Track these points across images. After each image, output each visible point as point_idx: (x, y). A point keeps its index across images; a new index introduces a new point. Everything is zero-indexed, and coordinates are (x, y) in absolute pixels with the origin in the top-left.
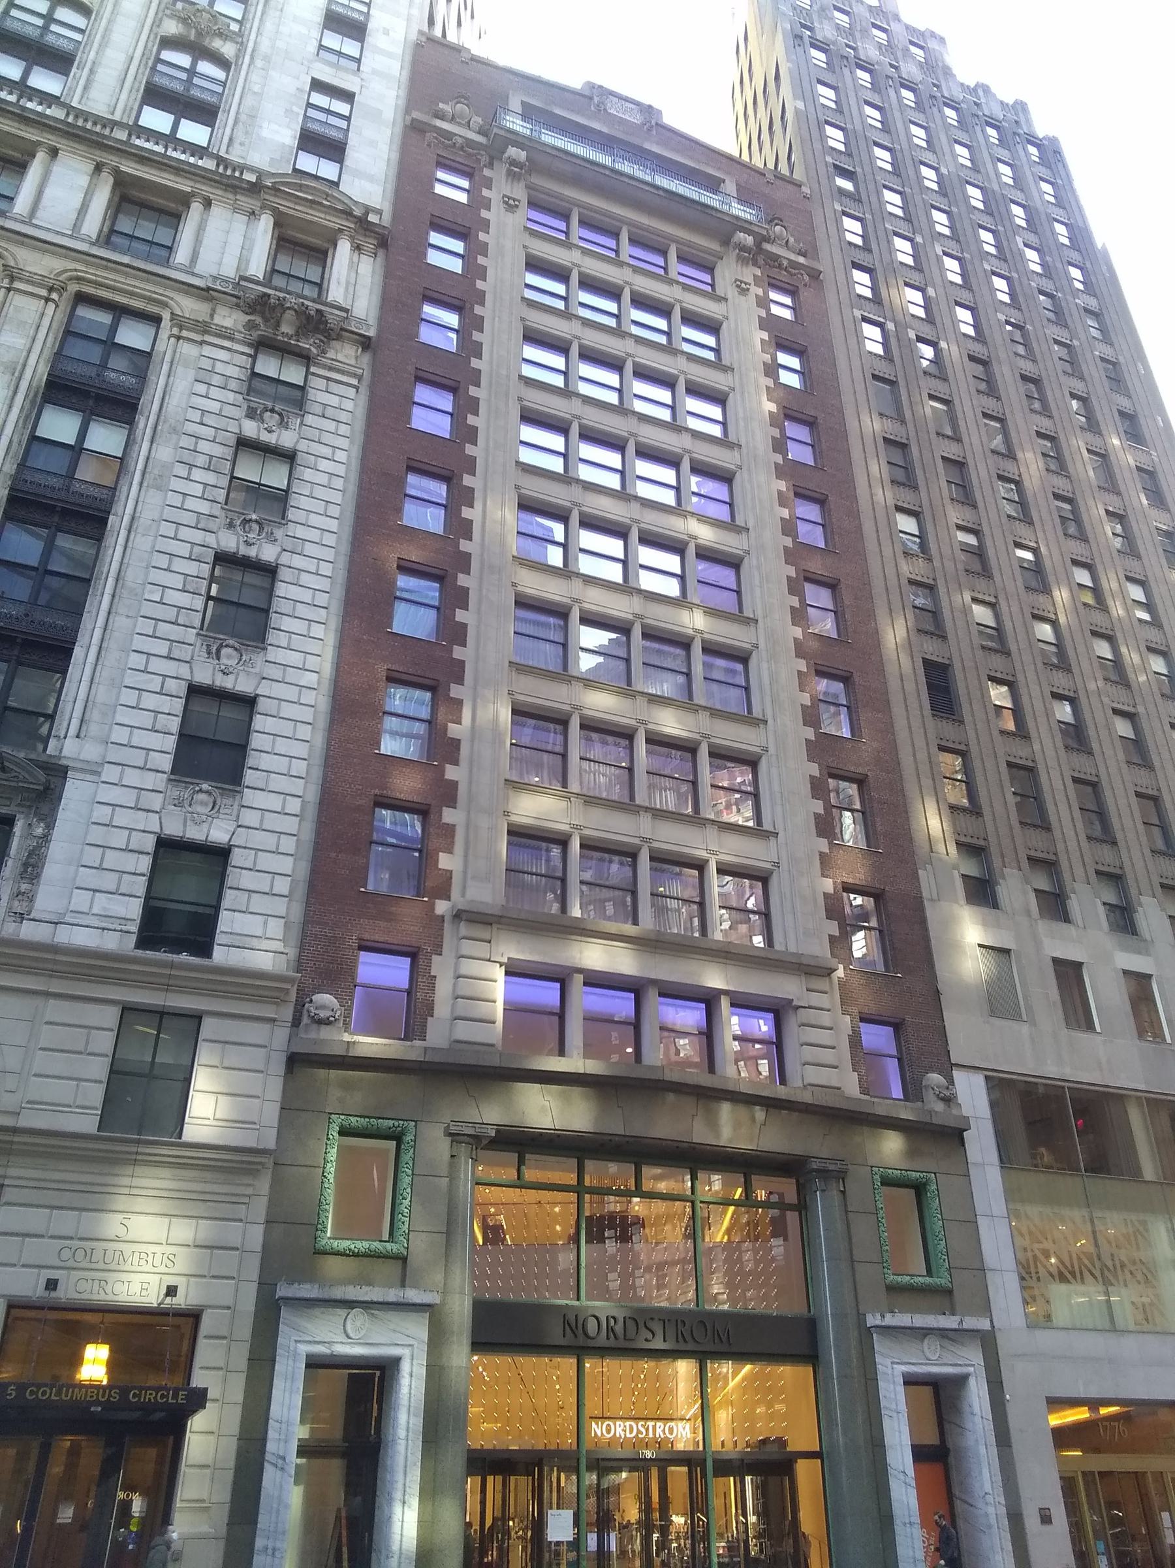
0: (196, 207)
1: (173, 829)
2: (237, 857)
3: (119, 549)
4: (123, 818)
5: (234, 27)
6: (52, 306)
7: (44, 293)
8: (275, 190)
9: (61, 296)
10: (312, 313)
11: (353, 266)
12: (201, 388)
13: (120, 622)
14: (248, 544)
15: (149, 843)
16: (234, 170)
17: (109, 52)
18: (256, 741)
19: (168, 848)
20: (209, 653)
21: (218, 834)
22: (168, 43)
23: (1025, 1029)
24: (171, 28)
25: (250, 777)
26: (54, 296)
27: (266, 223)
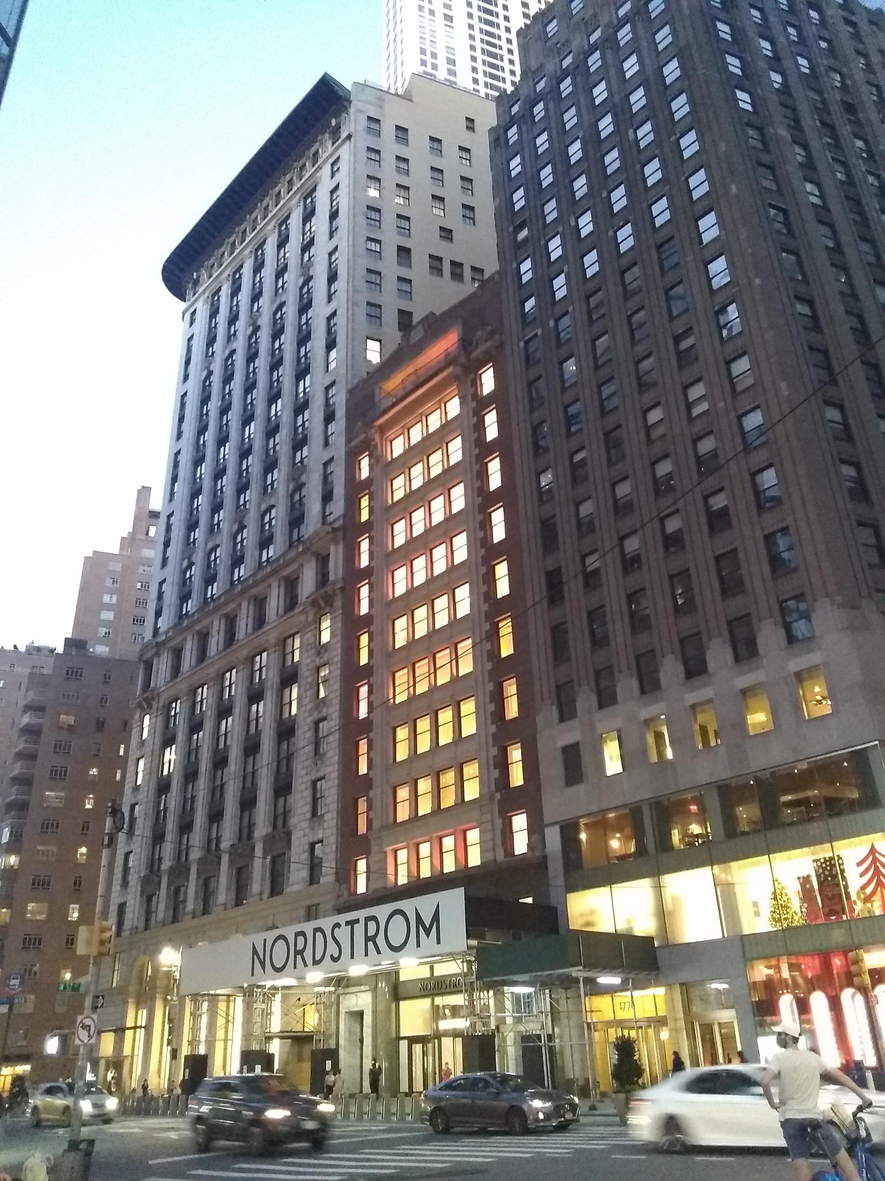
7: (274, 649)
24: (291, 487)
27: (314, 560)
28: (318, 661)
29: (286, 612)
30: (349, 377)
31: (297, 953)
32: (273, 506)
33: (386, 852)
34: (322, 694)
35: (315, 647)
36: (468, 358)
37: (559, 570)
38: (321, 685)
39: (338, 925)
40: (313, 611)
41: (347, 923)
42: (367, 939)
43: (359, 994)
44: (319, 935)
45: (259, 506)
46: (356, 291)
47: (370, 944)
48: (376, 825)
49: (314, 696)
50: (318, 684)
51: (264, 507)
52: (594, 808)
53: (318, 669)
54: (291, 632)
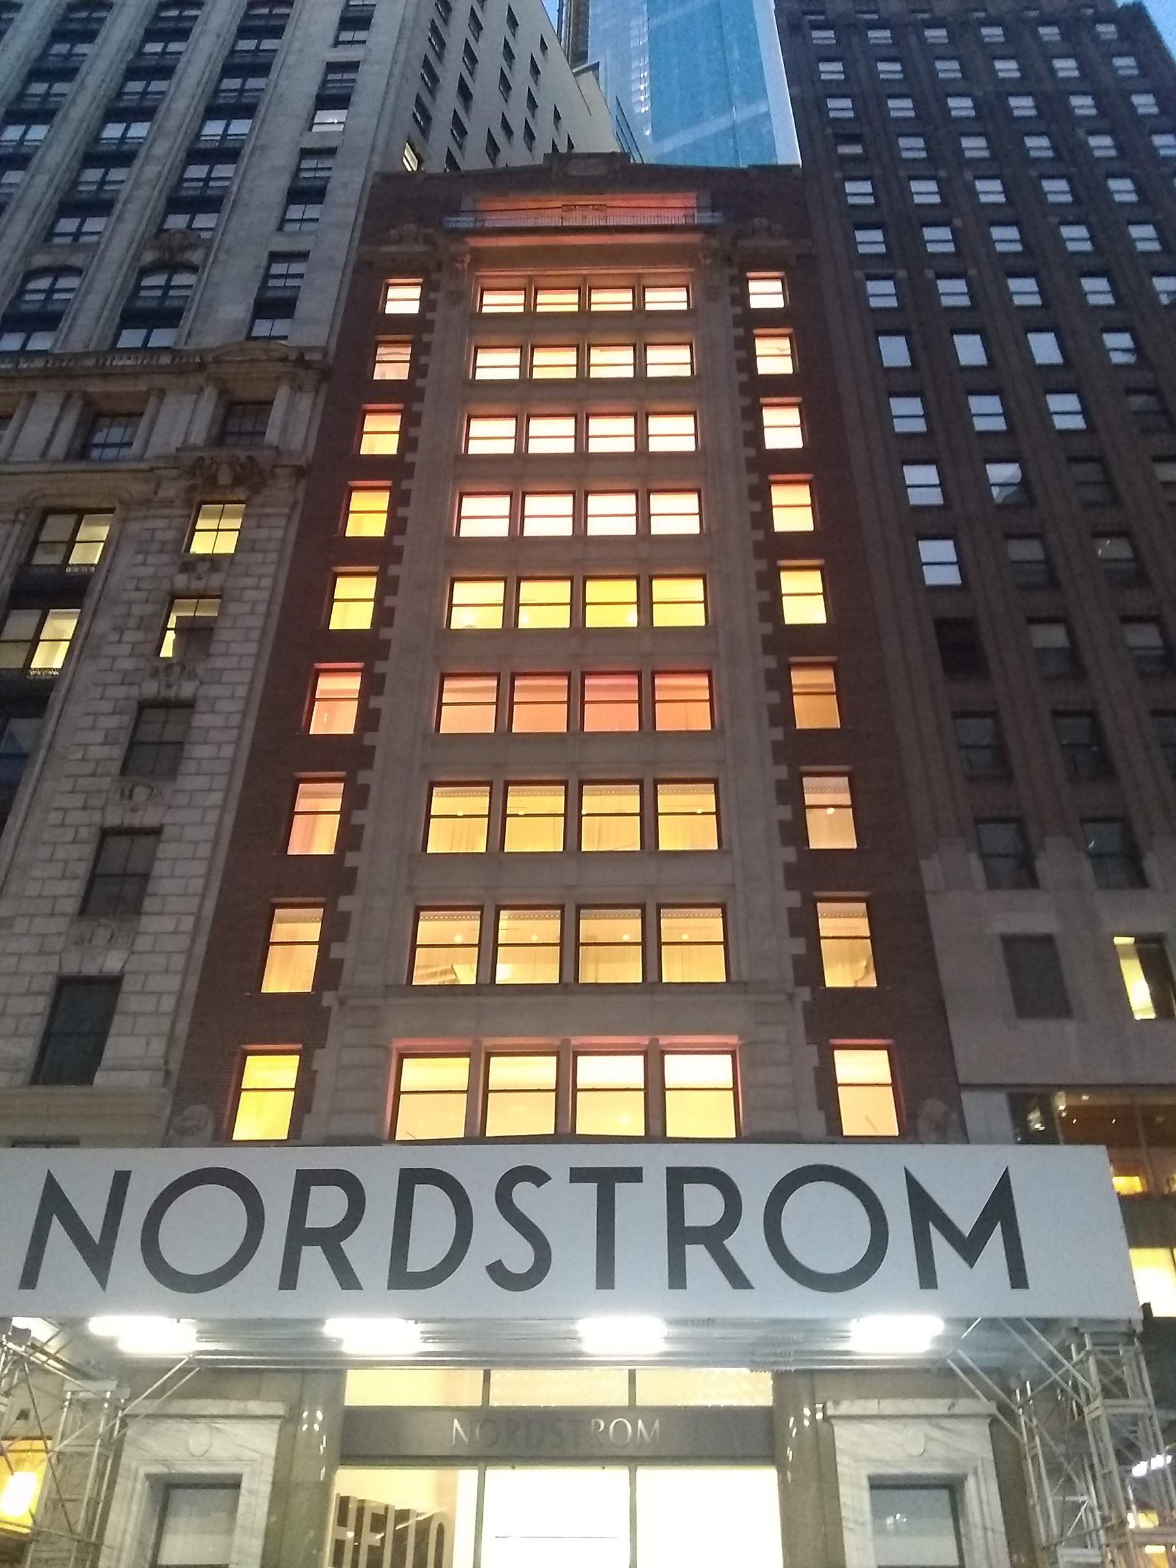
0: (153, 400)
1: (71, 967)
2: (129, 984)
3: (54, 720)
4: (27, 965)
5: (205, 235)
6: (18, 527)
7: (12, 517)
8: (217, 361)
9: (27, 515)
10: (243, 459)
11: (291, 405)
12: (140, 558)
13: (48, 785)
14: (169, 686)
15: (48, 983)
16: (189, 358)
17: (90, 298)
18: (160, 868)
19: (66, 985)
20: (122, 795)
21: (112, 963)
22: (145, 272)
23: (1070, 1028)
24: (148, 257)
25: (148, 904)
26: (21, 517)
27: (210, 393)
28: (181, 581)
29: (68, 456)
30: (377, 159)
31: (299, 1235)
32: (77, 271)
33: (388, 1050)
34: (167, 651)
35: (177, 551)
36: (734, 244)
37: (969, 623)
38: (170, 636)
39: (538, 1177)
40: (183, 484)
41: (578, 1175)
42: (680, 1235)
43: (221, 1425)
44: (431, 1203)
45: (28, 254)
46: (407, 63)
47: (696, 1254)
48: (359, 975)
49: (149, 649)
50: (165, 629)
51: (41, 260)
52: (1108, 1074)
53: (173, 598)
54: (82, 503)
